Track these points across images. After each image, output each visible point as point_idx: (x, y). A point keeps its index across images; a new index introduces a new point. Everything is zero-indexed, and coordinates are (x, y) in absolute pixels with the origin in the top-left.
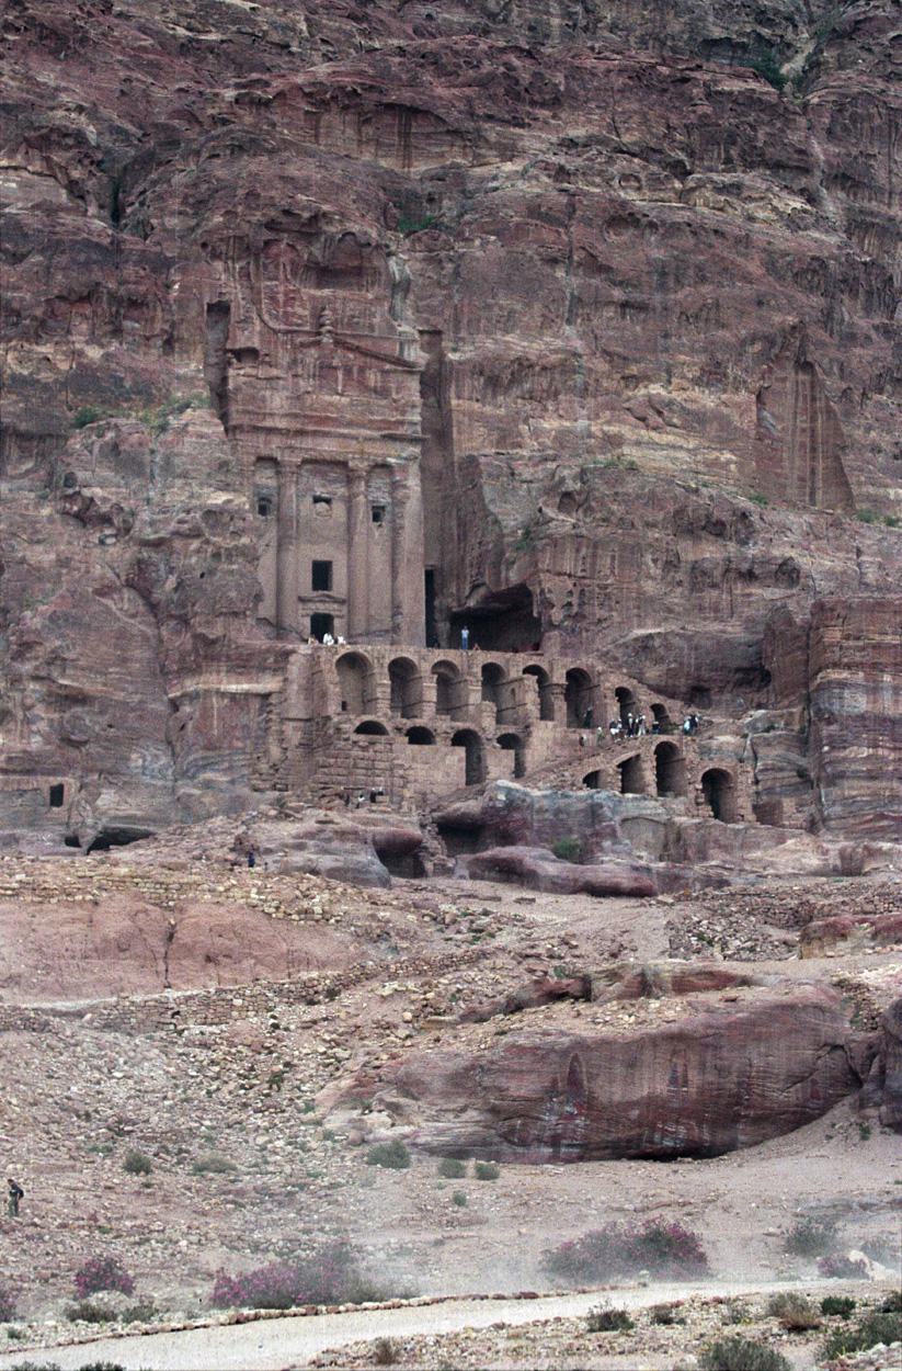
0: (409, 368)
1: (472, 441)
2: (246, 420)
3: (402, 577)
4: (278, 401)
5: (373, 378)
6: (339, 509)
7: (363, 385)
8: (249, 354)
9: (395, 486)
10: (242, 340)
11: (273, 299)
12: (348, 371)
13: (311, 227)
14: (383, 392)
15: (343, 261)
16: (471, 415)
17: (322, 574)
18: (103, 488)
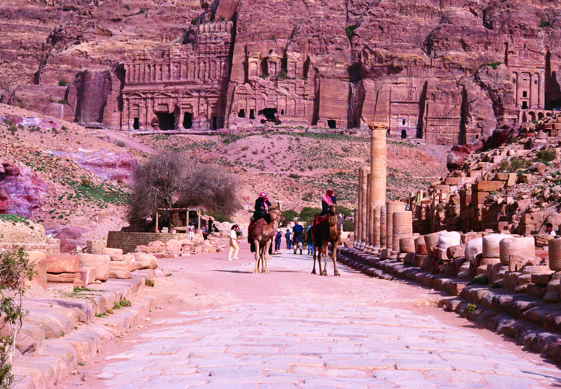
0: (542, 54)
2: (511, 65)
3: (541, 94)
4: (516, 61)
5: (535, 56)
6: (528, 81)
7: (534, 58)
8: (512, 52)
9: (539, 77)
10: (510, 49)
11: (516, 41)
12: (530, 55)
13: (523, 27)
14: (537, 59)
15: (529, 33)
16: (554, 63)
17: (525, 94)
18: (484, 79)
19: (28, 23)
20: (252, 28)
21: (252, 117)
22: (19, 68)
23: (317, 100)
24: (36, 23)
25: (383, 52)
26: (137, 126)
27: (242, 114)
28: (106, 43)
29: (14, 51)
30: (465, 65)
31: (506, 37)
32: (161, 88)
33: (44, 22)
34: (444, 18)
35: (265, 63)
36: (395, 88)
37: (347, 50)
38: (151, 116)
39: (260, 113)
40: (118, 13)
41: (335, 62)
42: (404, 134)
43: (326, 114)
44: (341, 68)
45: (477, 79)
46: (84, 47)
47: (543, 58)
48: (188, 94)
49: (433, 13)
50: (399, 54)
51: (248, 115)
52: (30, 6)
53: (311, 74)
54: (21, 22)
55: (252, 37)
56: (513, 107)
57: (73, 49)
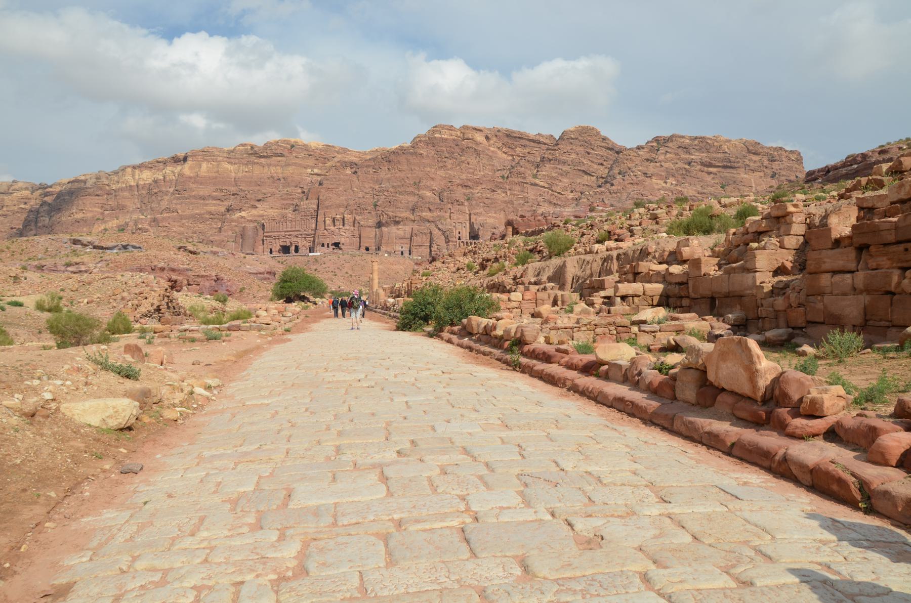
1: (473, 220)
18: (440, 226)
20: (327, 203)
22: (210, 224)
23: (360, 238)
24: (218, 202)
25: (391, 214)
26: (271, 252)
27: (323, 245)
28: (254, 212)
30: (431, 219)
31: (450, 206)
32: (283, 234)
34: (420, 197)
36: (397, 231)
37: (373, 213)
38: (278, 248)
40: (260, 197)
41: (368, 219)
42: (402, 253)
43: (364, 245)
44: (372, 222)
45: (436, 226)
46: (243, 214)
47: (468, 216)
48: (296, 236)
49: (415, 194)
50: (399, 214)
53: (357, 225)
55: (327, 208)
56: (454, 239)
57: (238, 214)
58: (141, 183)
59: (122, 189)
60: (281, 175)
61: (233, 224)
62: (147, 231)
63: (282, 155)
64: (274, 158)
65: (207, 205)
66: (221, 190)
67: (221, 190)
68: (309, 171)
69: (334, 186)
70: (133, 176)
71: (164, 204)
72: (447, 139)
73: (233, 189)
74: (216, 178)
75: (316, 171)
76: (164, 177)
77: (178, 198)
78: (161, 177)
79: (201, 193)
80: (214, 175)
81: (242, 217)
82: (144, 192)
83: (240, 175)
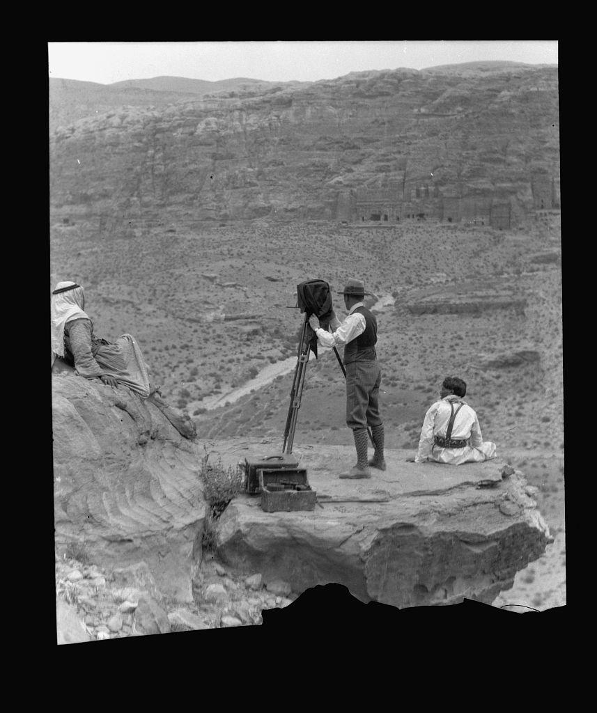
18: (520, 197)
19: (318, 152)
20: (413, 176)
21: (413, 217)
27: (409, 216)
28: (350, 176)
29: (312, 168)
33: (326, 150)
35: (418, 191)
39: (417, 216)
46: (340, 179)
51: (411, 216)
52: (319, 143)
54: (315, 152)
58: (248, 129)
59: (229, 136)
60: (386, 119)
61: (331, 190)
62: (255, 185)
63: (388, 94)
64: (380, 98)
65: (310, 156)
66: (325, 138)
67: (325, 138)
68: (416, 110)
69: (419, 156)
70: (240, 120)
71: (270, 155)
72: (543, 93)
73: (337, 137)
74: (320, 124)
75: (423, 110)
76: (270, 124)
77: (284, 150)
78: (267, 125)
79: (306, 143)
80: (317, 121)
81: (340, 183)
82: (251, 140)
83: (345, 120)
